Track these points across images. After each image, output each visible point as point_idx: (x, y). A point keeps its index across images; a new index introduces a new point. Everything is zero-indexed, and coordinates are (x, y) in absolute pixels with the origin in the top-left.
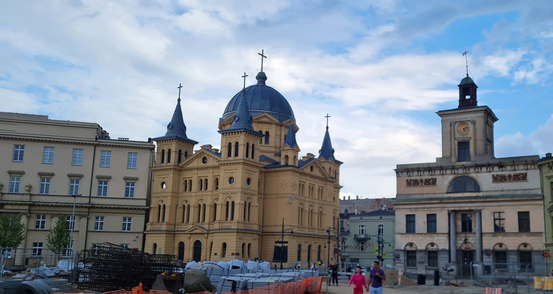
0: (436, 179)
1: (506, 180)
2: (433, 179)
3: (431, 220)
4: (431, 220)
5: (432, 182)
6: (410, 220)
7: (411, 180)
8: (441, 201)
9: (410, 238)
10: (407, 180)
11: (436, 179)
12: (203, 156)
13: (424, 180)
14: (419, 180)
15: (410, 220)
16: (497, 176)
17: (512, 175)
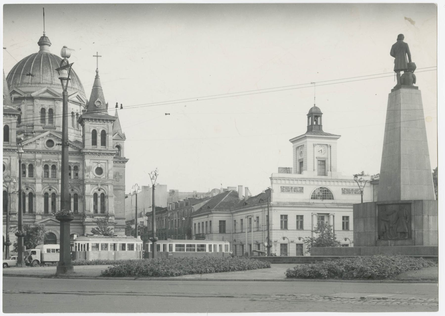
0: (302, 188)
1: (350, 193)
2: (300, 187)
3: (300, 218)
4: (300, 218)
5: (301, 190)
6: (284, 218)
7: (283, 187)
8: (307, 205)
9: (284, 233)
10: (281, 187)
11: (302, 188)
12: (48, 139)
13: (294, 188)
14: (290, 188)
15: (284, 218)
16: (345, 189)
17: (354, 189)
